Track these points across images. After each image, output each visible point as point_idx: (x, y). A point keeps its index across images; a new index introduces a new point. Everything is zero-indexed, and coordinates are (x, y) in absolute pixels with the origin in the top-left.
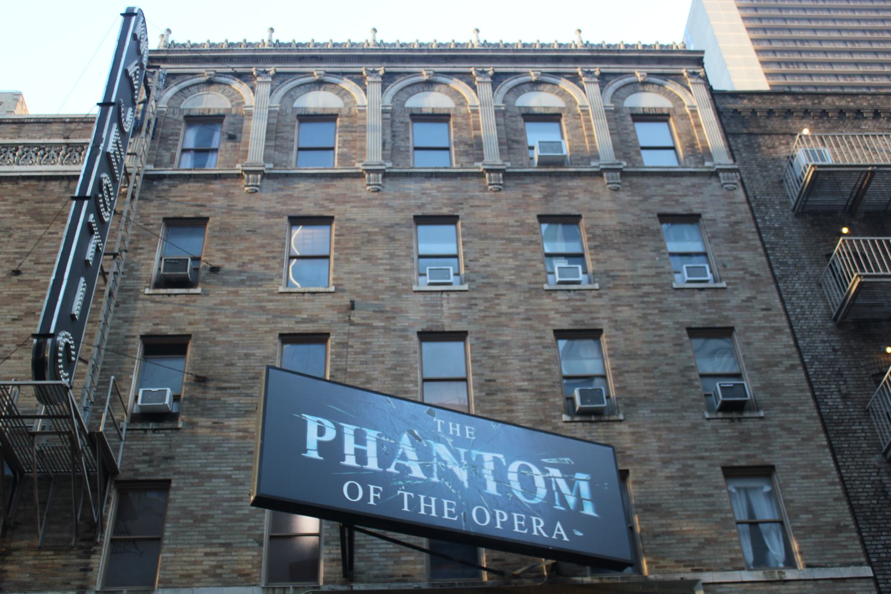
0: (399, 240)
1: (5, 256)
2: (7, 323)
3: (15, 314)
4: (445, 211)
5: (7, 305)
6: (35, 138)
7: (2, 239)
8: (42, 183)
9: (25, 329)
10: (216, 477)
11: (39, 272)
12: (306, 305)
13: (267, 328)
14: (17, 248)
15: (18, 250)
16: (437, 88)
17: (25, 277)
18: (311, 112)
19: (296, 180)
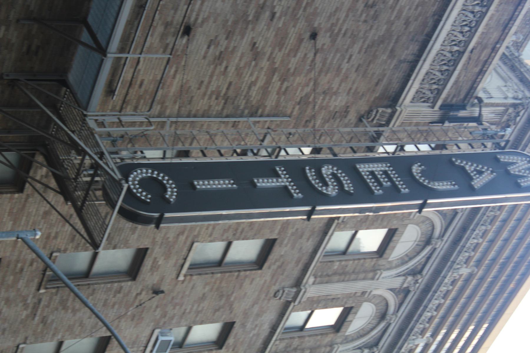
0: (214, 315)
1: (341, 22)
2: (253, 38)
3: (260, 45)
4: (231, 341)
5: (276, 35)
6: (491, 18)
7: (364, 15)
8: (421, 38)
9: (239, 54)
10: (14, 224)
11: (306, 55)
12: (172, 262)
13: (159, 239)
14: (346, 30)
15: (343, 32)
16: (375, 322)
17: (307, 44)
18: (395, 238)
19: (318, 239)
